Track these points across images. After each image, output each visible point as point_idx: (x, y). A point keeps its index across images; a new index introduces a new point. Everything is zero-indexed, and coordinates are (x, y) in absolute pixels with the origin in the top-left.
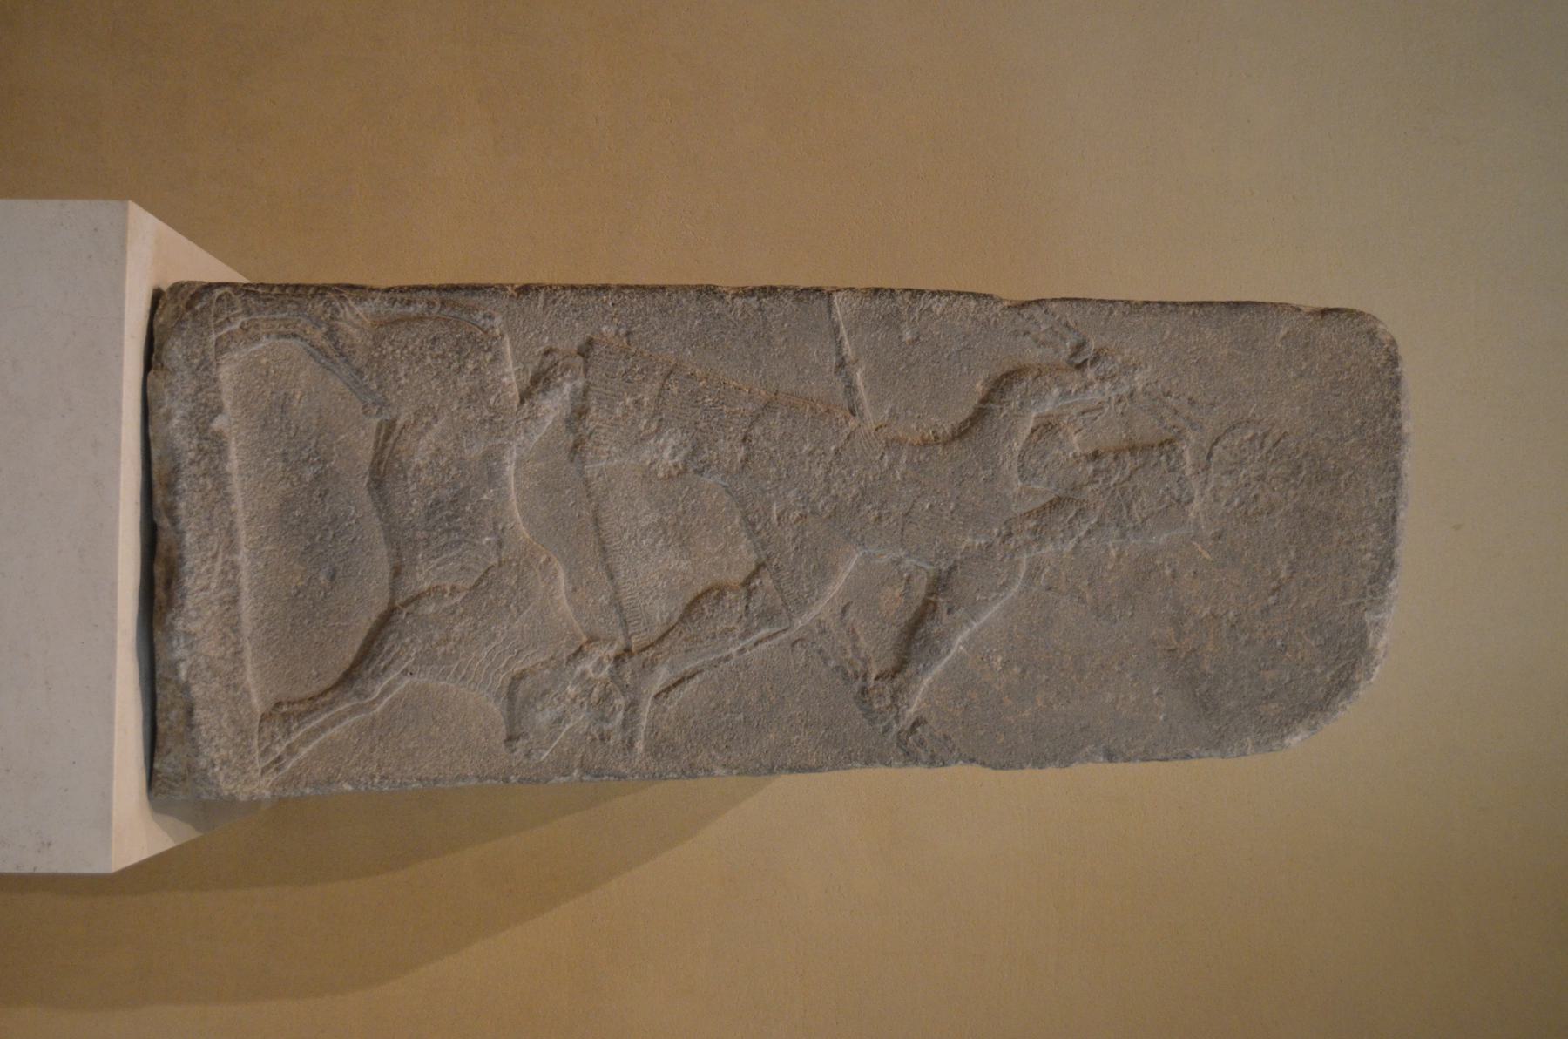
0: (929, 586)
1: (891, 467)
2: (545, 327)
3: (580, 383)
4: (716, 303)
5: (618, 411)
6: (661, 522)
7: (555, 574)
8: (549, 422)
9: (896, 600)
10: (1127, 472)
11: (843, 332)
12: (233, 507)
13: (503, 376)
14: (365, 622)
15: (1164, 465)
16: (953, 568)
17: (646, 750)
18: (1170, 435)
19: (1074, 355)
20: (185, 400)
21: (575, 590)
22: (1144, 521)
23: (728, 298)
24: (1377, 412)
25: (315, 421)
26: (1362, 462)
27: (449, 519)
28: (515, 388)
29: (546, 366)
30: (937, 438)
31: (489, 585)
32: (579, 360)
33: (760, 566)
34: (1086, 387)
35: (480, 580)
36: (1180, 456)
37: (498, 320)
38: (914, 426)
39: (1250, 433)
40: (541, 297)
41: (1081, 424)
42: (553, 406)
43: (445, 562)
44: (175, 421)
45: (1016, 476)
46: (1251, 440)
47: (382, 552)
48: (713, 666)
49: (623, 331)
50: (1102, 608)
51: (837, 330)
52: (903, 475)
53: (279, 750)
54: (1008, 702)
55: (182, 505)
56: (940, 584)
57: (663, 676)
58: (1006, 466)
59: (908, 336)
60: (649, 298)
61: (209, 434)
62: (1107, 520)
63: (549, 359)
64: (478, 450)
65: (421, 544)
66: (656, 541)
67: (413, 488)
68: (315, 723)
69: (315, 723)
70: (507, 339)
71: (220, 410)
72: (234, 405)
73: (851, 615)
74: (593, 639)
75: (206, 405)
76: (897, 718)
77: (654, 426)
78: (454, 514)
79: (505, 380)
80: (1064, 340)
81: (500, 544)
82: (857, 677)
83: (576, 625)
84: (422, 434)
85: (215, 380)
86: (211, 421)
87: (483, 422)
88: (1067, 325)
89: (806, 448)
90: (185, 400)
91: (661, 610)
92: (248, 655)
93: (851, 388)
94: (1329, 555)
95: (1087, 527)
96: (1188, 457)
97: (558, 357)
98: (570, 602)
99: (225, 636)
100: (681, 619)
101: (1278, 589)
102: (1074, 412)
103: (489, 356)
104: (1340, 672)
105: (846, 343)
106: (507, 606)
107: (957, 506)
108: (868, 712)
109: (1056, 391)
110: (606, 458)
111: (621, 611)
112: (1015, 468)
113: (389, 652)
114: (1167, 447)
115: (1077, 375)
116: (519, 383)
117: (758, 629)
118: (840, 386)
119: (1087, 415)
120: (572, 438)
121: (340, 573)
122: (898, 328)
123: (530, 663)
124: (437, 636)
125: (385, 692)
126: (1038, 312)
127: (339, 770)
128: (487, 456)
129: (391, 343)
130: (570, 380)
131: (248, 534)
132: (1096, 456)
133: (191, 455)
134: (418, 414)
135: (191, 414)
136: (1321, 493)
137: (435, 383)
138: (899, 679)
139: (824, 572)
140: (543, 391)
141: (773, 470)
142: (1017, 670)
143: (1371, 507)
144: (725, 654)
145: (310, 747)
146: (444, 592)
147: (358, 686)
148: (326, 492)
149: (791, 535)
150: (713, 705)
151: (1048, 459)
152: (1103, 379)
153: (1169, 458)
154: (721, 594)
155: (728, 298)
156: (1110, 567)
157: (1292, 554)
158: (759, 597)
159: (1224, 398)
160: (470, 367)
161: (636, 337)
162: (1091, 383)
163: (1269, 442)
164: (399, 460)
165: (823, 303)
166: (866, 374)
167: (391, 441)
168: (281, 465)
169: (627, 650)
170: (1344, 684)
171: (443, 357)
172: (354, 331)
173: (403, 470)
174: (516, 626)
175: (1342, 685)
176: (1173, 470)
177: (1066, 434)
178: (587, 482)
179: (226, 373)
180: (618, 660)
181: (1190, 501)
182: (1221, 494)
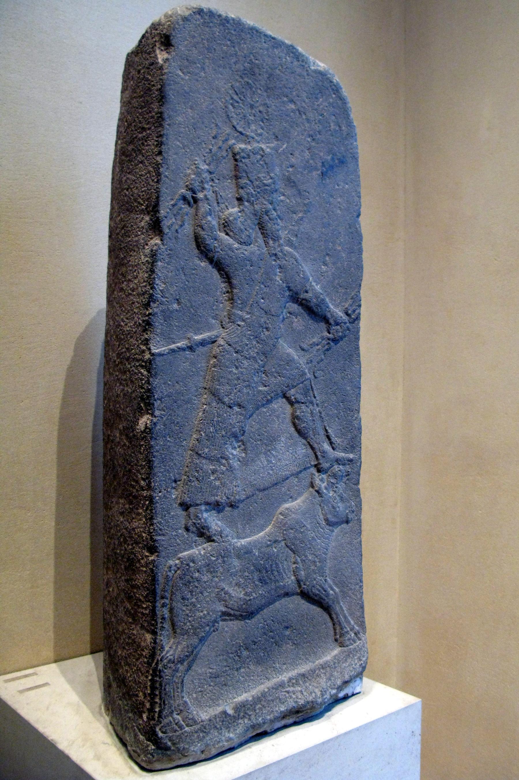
0: (293, 302)
1: (244, 320)
2: (174, 533)
3: (203, 508)
4: (158, 427)
5: (217, 483)
6: (265, 453)
7: (287, 509)
8: (219, 523)
9: (299, 321)
10: (248, 182)
11: (173, 346)
12: (266, 690)
13: (200, 554)
14: (304, 605)
15: (247, 161)
16: (290, 289)
17: (352, 453)
18: (230, 155)
19: (189, 204)
20: (221, 734)
21: (291, 497)
22: (271, 178)
23: (155, 420)
24: (225, 30)
25: (221, 657)
26: (248, 47)
27: (267, 572)
28: (205, 545)
29: (195, 529)
30: (228, 292)
31: (294, 544)
32: (192, 510)
33: (285, 396)
34: (207, 199)
35: (291, 550)
36: (243, 150)
37: (171, 562)
38: (221, 305)
39: (231, 107)
40: (158, 538)
41: (223, 206)
42: (214, 522)
43: (284, 569)
44: (231, 735)
45: (249, 247)
46: (234, 107)
47: (277, 604)
49: (174, 485)
50: (305, 209)
51: (173, 351)
52: (248, 313)
53: (353, 635)
54: (339, 265)
55: (268, 717)
56: (295, 298)
57: (326, 447)
58: (246, 253)
59: (175, 306)
60: (156, 470)
61: (236, 715)
62: (270, 198)
63: (191, 528)
64: (236, 562)
65: (277, 584)
66: (273, 455)
67: (254, 595)
70: (180, 555)
71: (225, 713)
72: (218, 705)
73: (305, 346)
74: (312, 485)
75: (223, 721)
76: (345, 323)
77: (224, 461)
78: (263, 569)
79: (202, 553)
80: (181, 209)
81: (276, 541)
82: (329, 343)
83: (306, 495)
84: (230, 596)
85: (210, 720)
86: (230, 715)
87: (224, 562)
88: (173, 205)
89: (234, 370)
90: (221, 734)
91: (302, 450)
92: (321, 661)
93: (203, 343)
94: (287, 80)
95: (273, 212)
96: (243, 146)
97: (190, 523)
98: (296, 499)
99: (317, 676)
100: (305, 438)
101: (299, 111)
102: (217, 209)
103: (192, 564)
104: (333, 90)
105: (179, 345)
106: (302, 533)
107: (263, 283)
108: (341, 338)
109: (209, 218)
110: (237, 489)
111: (301, 471)
112: (246, 247)
114: (238, 157)
115: (200, 204)
116: (202, 543)
118: (201, 350)
119: (219, 201)
120: (227, 509)
121: (286, 624)
122: (172, 312)
123: (322, 516)
124: (312, 567)
125: (332, 589)
128: (239, 557)
129: (185, 624)
130: (202, 514)
131: (274, 678)
132: (240, 199)
133: (246, 721)
134: (220, 600)
135: (228, 728)
136: (260, 75)
138: (332, 321)
139: (290, 361)
140: (208, 528)
141: (245, 391)
142: (327, 258)
143: (267, 50)
145: (350, 619)
146: (296, 567)
147: (330, 603)
148: (253, 641)
149: (273, 379)
150: (337, 419)
151: (242, 227)
152: (203, 188)
153: (244, 158)
154: (297, 418)
155: (155, 420)
156: (288, 201)
157: (285, 99)
158: (300, 397)
159: (214, 118)
160: (197, 575)
161: (177, 476)
162: (205, 196)
163: (235, 97)
164: (242, 605)
165: (158, 358)
166: (196, 334)
167: (232, 612)
168: (242, 670)
169: (316, 466)
171: (191, 592)
172: (180, 648)
173: (246, 602)
174: (308, 526)
175: (337, 91)
176: (249, 156)
177: (230, 215)
178: (247, 498)
179: (204, 715)
180: (319, 471)
181: (262, 150)
182: (259, 132)
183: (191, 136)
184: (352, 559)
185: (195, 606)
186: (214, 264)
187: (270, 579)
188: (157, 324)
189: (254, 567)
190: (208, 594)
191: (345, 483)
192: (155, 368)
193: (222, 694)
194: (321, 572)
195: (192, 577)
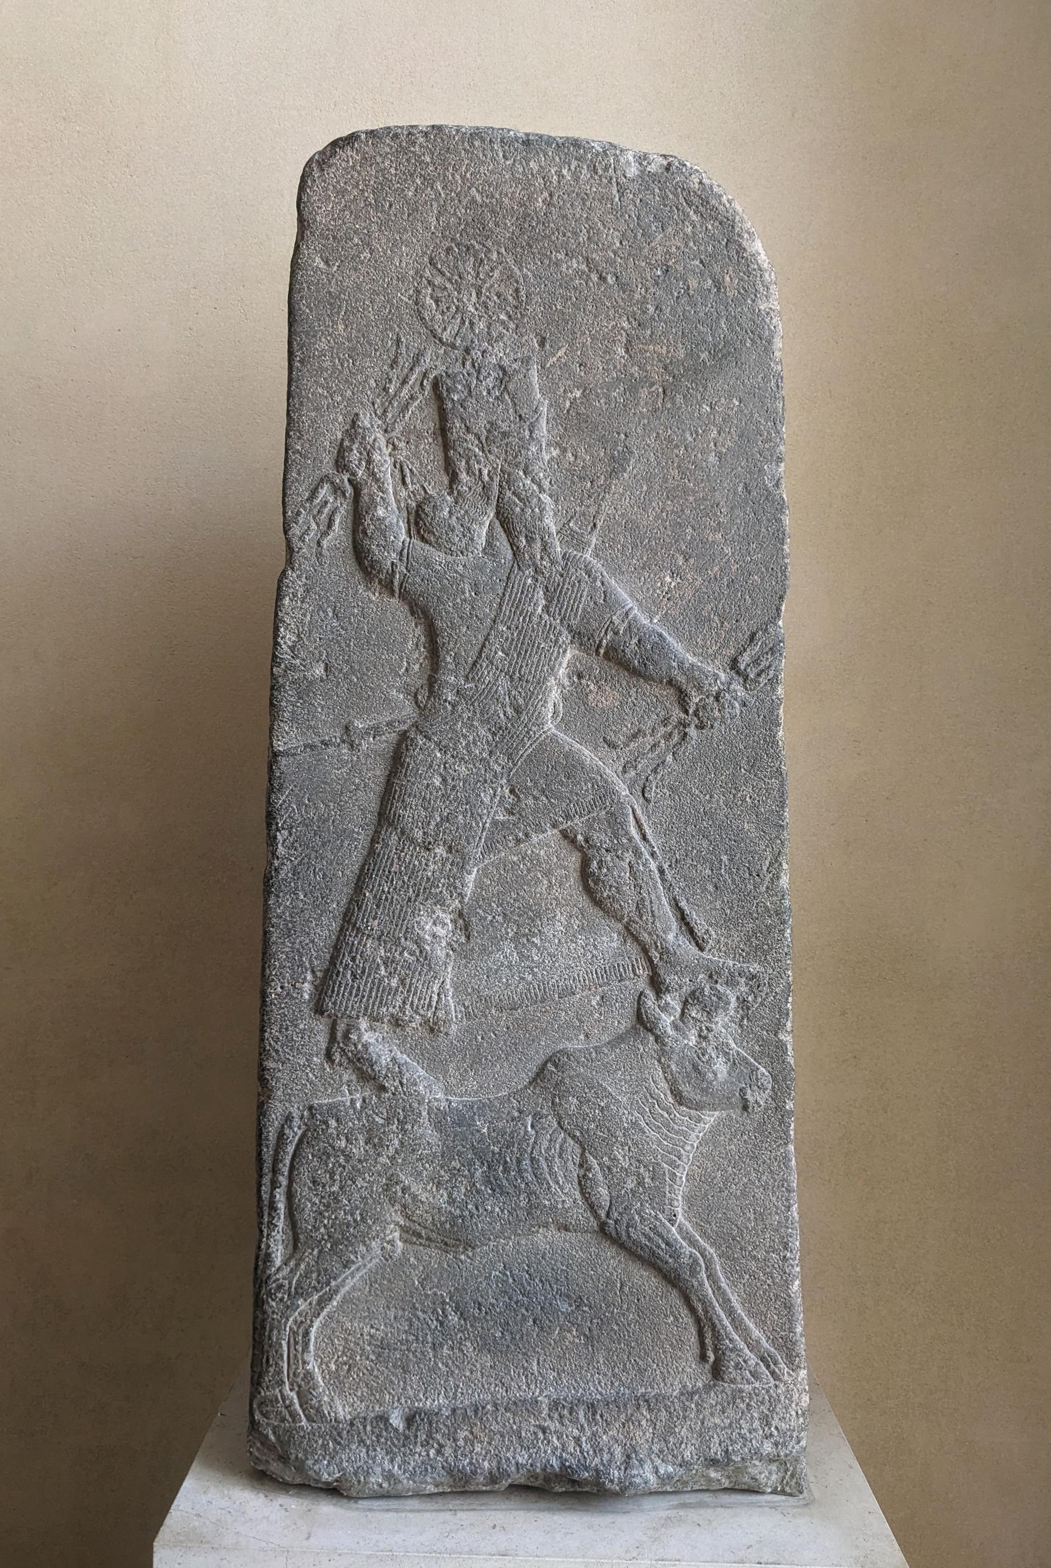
27: (506, 1170)
48: (669, 888)
68: (726, 1322)
69: (726, 1322)
84: (414, 1197)
113: (650, 1239)
117: (630, 839)
122: (311, 683)
123: (664, 1085)
125: (692, 1243)
126: (296, 530)
127: (777, 1296)
137: (360, 1182)
144: (657, 875)
170: (704, 201)
174: (624, 1100)
183: (346, 372)
184: (759, 1193)
185: (337, 1200)
186: (397, 595)
187: (515, 1187)
188: (284, 704)
189: (475, 1154)
190: (366, 1184)
191: (741, 1026)
192: (279, 777)
193: (391, 1382)
194: (658, 1197)
195: (333, 1148)
